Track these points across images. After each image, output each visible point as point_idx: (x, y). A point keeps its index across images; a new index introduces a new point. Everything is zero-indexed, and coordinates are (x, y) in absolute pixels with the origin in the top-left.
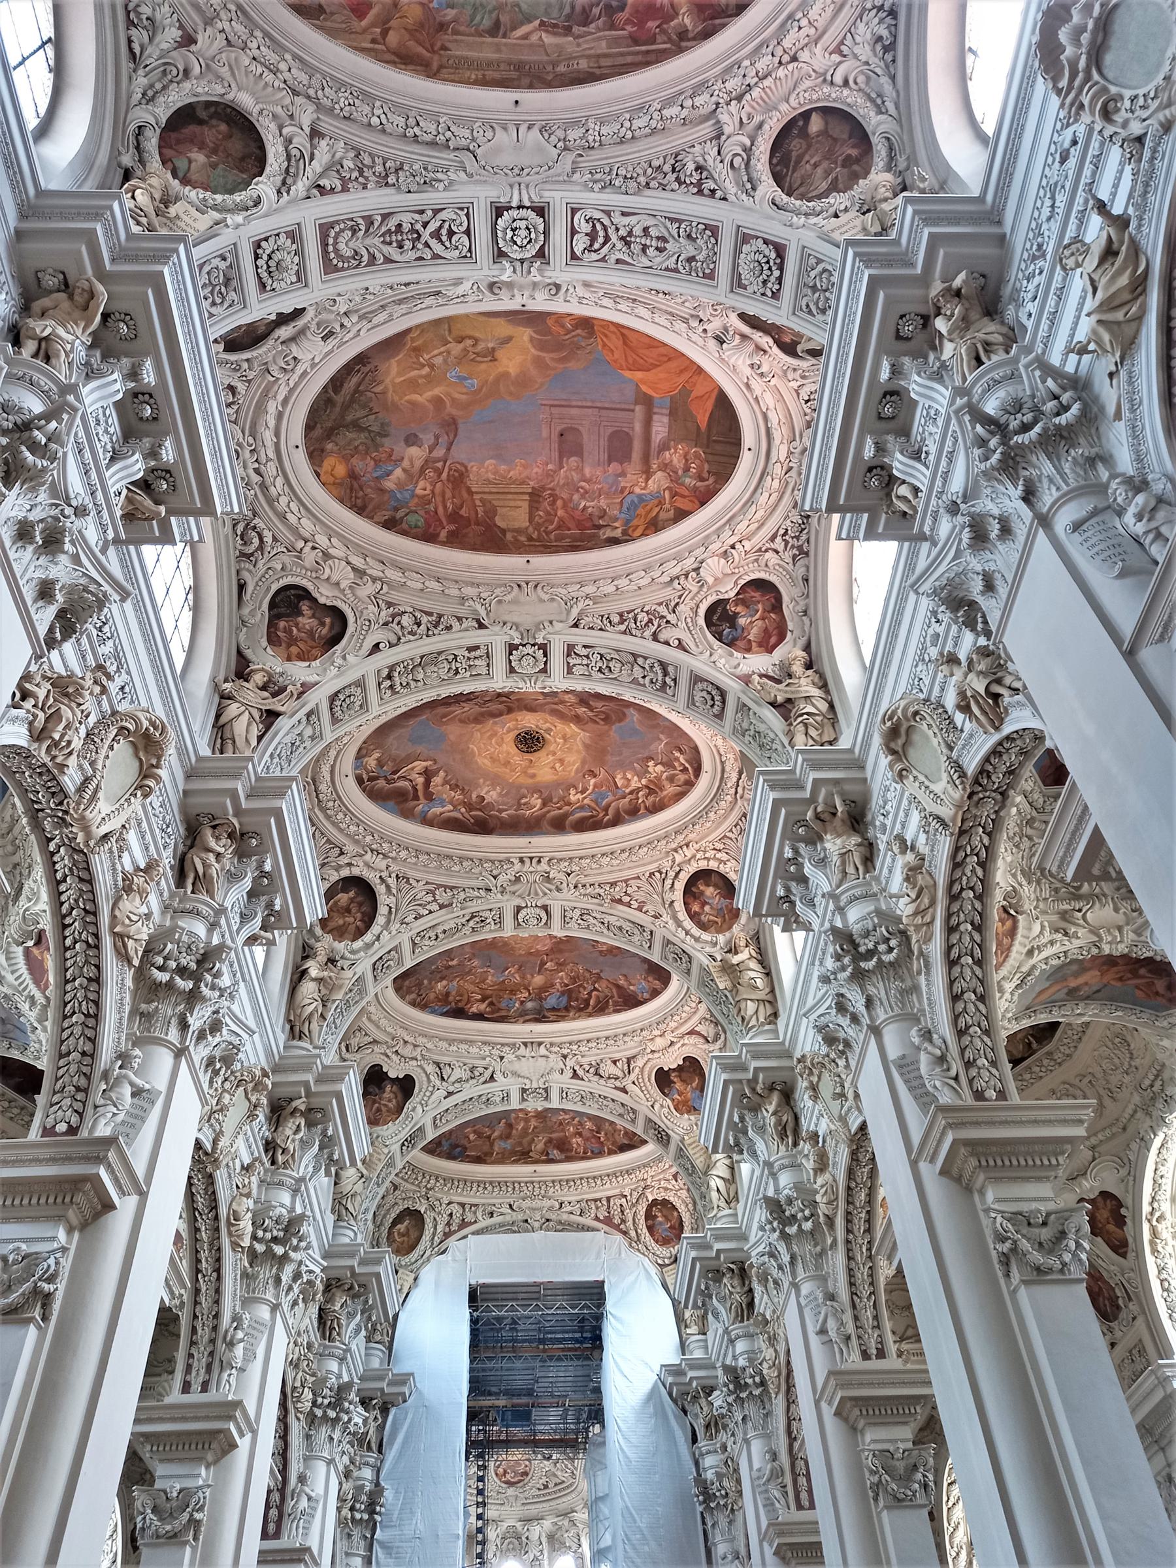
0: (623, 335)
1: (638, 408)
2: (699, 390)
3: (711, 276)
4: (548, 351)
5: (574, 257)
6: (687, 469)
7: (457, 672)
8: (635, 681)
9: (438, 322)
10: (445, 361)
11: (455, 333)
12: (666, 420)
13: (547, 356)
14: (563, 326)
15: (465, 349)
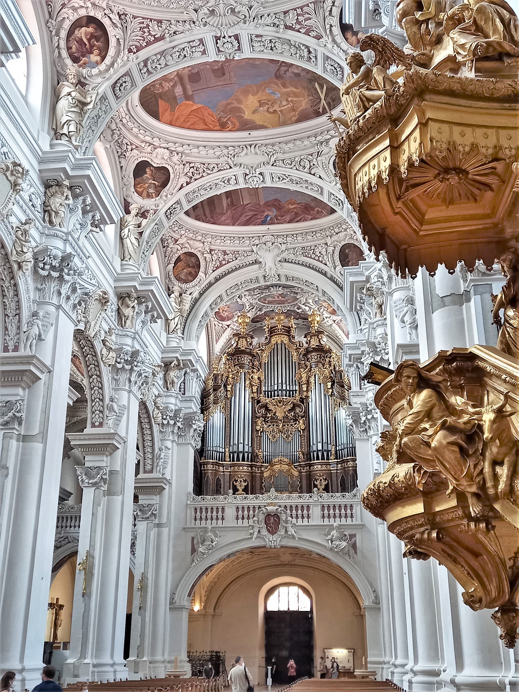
0: (206, 125)
1: (191, 93)
2: (168, 113)
3: (186, 195)
4: (236, 107)
5: (235, 175)
6: (161, 84)
7: (271, 41)
8: (162, 53)
9: (284, 124)
10: (281, 102)
11: (277, 116)
12: (177, 94)
13: (236, 105)
14: (232, 122)
15: (273, 107)
